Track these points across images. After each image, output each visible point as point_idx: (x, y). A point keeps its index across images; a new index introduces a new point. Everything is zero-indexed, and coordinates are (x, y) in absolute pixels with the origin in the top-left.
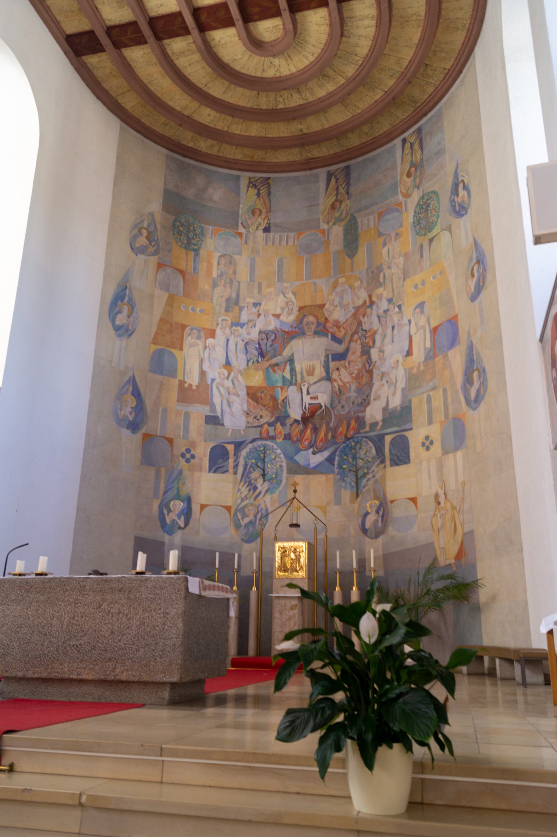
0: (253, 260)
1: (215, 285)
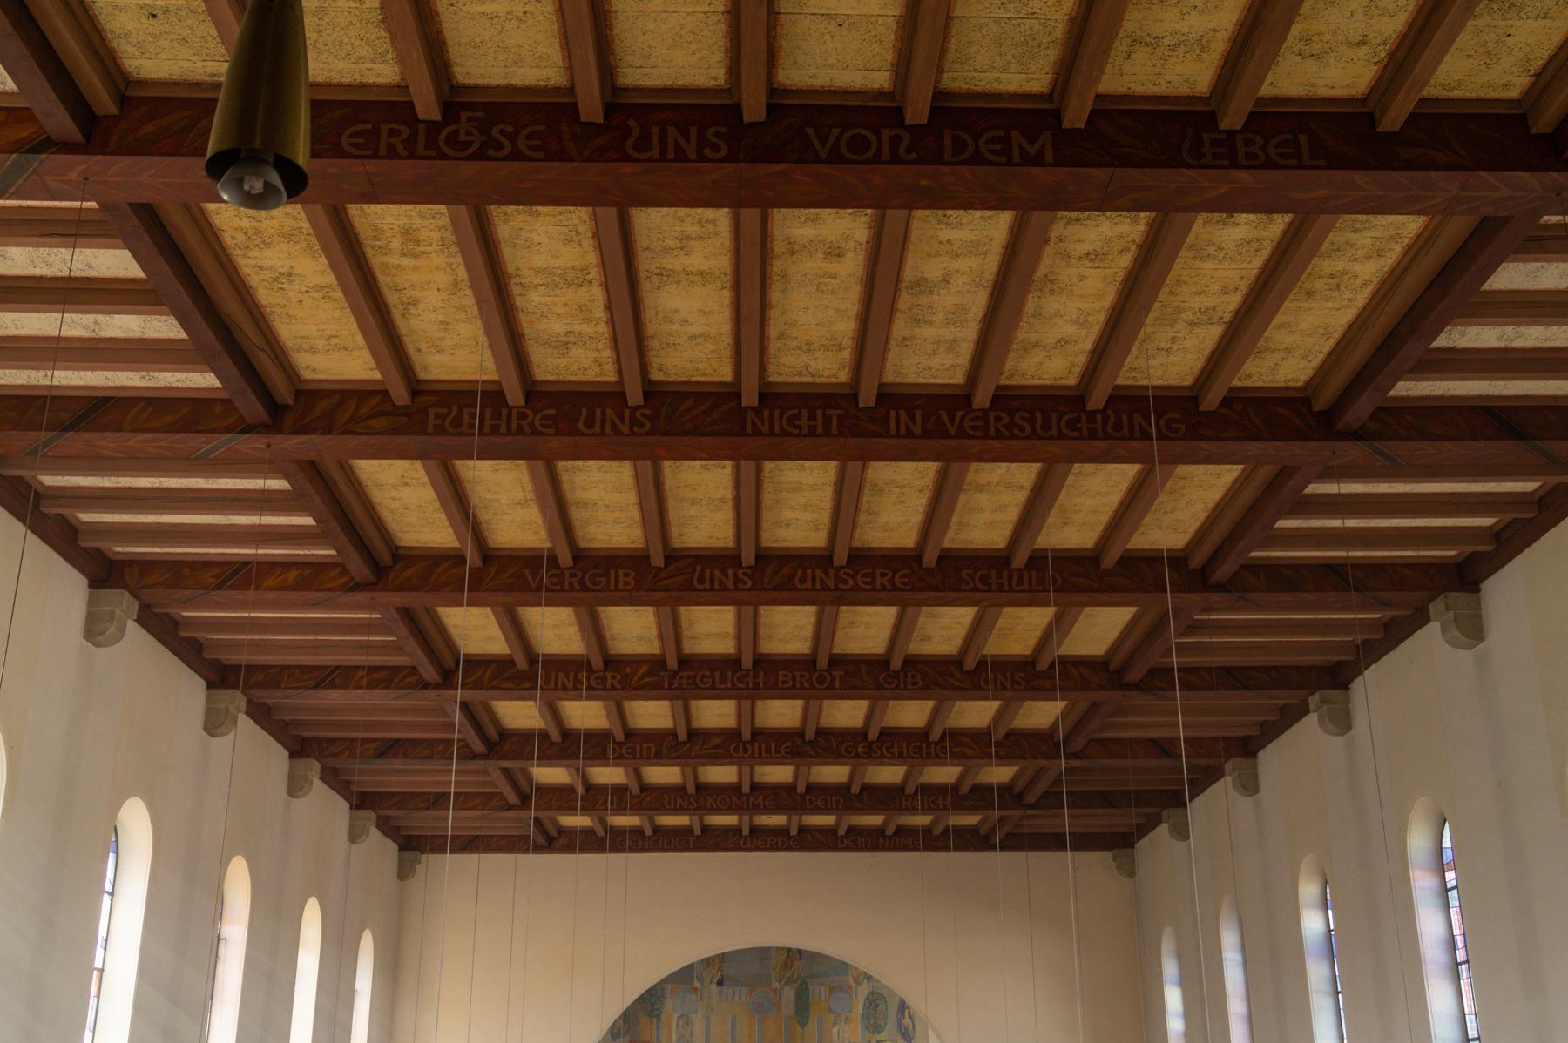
0: (708, 1019)
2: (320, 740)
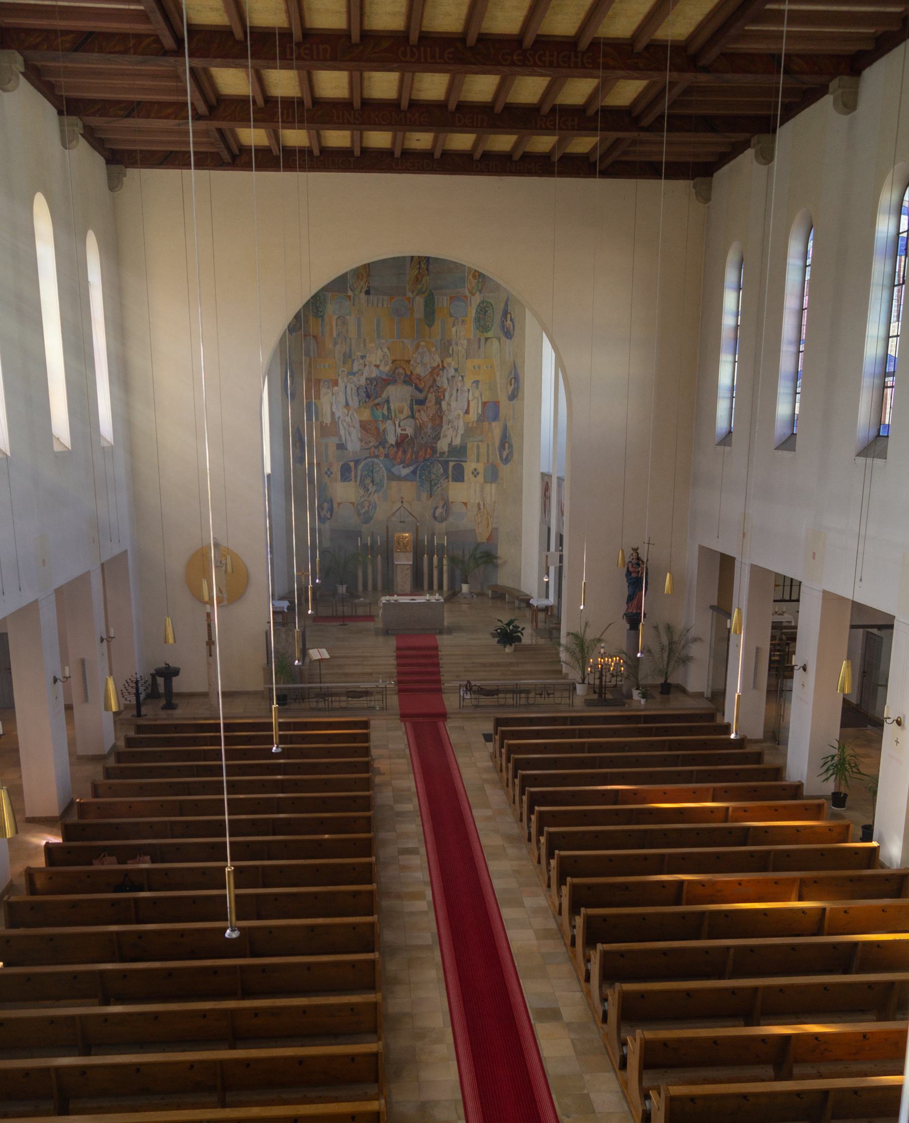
1: (335, 344)
2: (19, 30)
